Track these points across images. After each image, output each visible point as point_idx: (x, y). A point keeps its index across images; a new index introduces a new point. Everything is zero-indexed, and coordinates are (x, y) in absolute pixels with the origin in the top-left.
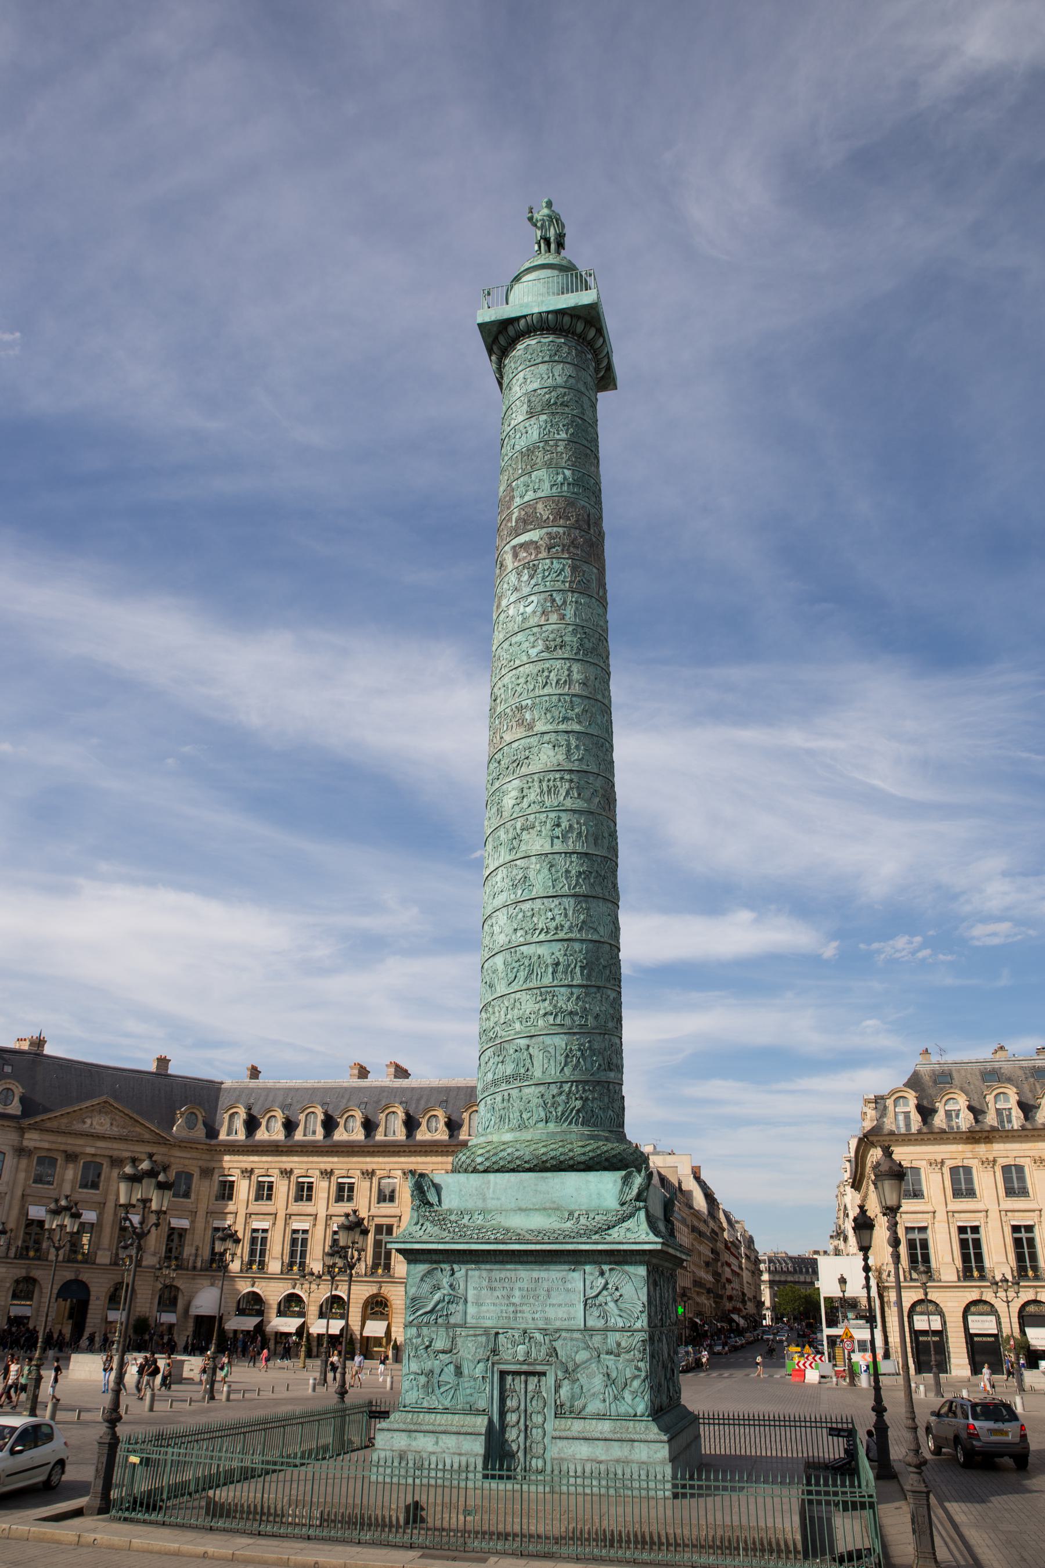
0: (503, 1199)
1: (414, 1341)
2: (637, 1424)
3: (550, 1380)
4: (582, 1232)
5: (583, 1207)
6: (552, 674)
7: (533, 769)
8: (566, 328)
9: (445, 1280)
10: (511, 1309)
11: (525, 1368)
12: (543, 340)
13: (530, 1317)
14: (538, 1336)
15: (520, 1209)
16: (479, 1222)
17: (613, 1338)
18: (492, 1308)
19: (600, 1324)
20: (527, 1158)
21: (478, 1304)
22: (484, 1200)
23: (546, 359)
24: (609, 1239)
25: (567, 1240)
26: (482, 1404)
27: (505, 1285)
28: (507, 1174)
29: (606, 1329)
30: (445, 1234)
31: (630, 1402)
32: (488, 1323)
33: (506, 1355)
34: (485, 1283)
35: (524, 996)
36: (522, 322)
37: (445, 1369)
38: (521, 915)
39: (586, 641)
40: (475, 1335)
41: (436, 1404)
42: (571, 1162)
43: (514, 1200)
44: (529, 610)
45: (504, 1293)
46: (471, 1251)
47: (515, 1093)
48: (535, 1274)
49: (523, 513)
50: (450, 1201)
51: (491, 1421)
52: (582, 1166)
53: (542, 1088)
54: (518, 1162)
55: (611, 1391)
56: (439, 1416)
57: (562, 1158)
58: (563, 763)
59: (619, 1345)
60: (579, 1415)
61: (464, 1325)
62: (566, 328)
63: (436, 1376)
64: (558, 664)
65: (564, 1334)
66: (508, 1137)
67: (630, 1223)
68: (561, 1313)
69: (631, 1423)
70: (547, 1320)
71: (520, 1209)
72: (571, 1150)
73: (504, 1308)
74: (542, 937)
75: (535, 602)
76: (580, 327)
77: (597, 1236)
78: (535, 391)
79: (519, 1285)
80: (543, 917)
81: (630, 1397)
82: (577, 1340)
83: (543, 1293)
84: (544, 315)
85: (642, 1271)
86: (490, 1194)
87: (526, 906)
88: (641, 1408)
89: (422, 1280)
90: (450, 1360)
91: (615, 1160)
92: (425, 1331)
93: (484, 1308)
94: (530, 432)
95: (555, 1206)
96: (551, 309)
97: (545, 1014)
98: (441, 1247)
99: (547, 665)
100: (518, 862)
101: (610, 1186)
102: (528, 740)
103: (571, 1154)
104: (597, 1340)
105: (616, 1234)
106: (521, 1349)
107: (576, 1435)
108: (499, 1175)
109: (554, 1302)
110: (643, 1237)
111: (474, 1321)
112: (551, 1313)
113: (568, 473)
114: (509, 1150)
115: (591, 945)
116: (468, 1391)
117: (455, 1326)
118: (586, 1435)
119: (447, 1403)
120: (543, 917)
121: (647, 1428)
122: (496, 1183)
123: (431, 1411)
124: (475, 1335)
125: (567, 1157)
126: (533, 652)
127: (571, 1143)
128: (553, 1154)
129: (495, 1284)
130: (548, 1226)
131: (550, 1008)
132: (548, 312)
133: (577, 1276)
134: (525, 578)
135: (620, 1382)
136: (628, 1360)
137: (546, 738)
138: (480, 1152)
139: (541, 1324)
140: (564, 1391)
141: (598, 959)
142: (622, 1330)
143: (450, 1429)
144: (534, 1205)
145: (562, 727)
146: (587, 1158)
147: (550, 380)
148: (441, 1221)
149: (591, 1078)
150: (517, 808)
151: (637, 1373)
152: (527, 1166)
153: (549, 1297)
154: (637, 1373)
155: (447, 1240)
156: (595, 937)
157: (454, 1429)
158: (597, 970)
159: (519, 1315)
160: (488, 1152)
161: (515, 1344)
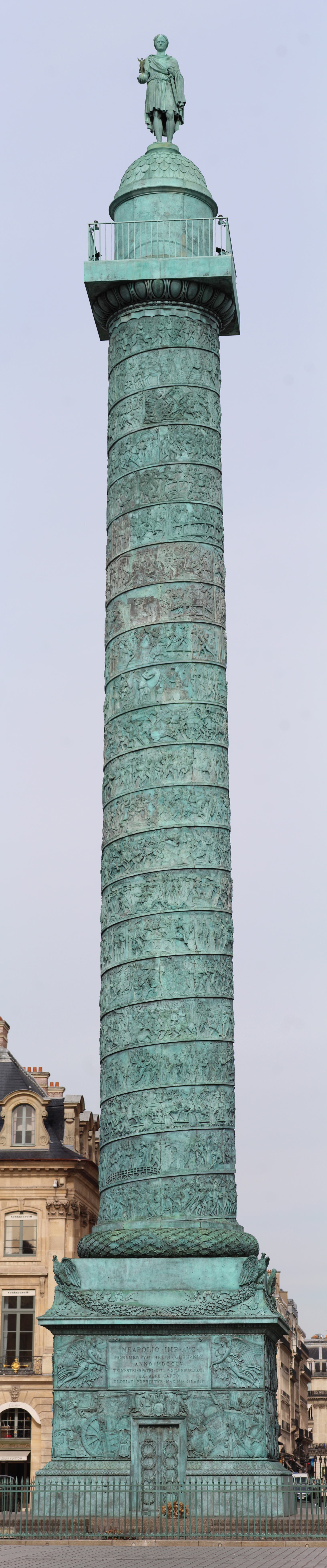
0: (138, 1280)
1: (63, 1403)
2: (255, 1463)
3: (182, 1431)
4: (210, 1309)
5: (209, 1288)
7: (157, 866)
8: (190, 298)
9: (90, 1351)
10: (148, 1374)
11: (160, 1422)
12: (163, 313)
13: (165, 1379)
14: (171, 1396)
15: (154, 1290)
16: (118, 1301)
17: (235, 1396)
18: (131, 1373)
19: (223, 1385)
20: (159, 1245)
21: (118, 1370)
22: (122, 1282)
23: (167, 343)
24: (232, 1314)
25: (198, 1315)
26: (124, 1453)
27: (143, 1354)
28: (141, 1260)
29: (229, 1389)
30: (89, 1311)
31: (249, 1446)
32: (129, 1386)
33: (146, 1411)
34: (125, 1353)
35: (151, 1095)
36: (141, 286)
37: (92, 1425)
38: (147, 1015)
39: (208, 720)
40: (117, 1397)
41: (84, 1454)
42: (197, 1249)
43: (148, 1282)
44: (151, 683)
45: (142, 1361)
46: (113, 1326)
47: (143, 1185)
48: (169, 1345)
50: (91, 1283)
51: (132, 1467)
52: (206, 1252)
53: (168, 1181)
54: (151, 1249)
55: (233, 1438)
56: (88, 1463)
57: (189, 1245)
58: (187, 862)
59: (240, 1401)
60: (207, 1458)
61: (106, 1389)
62: (190, 298)
63: (84, 1431)
65: (194, 1394)
66: (139, 1225)
67: (249, 1302)
68: (191, 1376)
69: (250, 1463)
70: (180, 1382)
71: (154, 1290)
72: (197, 1238)
73: (142, 1373)
74: (167, 1039)
75: (157, 675)
76: (206, 296)
77: (222, 1313)
79: (154, 1354)
80: (169, 1020)
81: (250, 1443)
82: (205, 1398)
83: (176, 1360)
84: (167, 283)
85: (260, 1340)
86: (126, 1276)
87: (152, 1007)
88: (259, 1450)
89: (68, 1351)
90: (96, 1417)
91: (233, 1246)
92: (72, 1394)
93: (125, 1374)
94: (149, 448)
95: (185, 1287)
96: (176, 276)
97: (170, 1114)
98: (87, 1322)
99: (170, 752)
100: (142, 963)
101: (233, 1270)
102: (152, 835)
103: (197, 1241)
104: (221, 1399)
105: (238, 1311)
106: (159, 1406)
107: (206, 1472)
108: (134, 1260)
109: (185, 1367)
110: (262, 1313)
111: (116, 1385)
112: (183, 1376)
113: (189, 507)
114: (142, 1238)
115: (211, 1046)
116: (113, 1442)
117: (99, 1389)
118: (216, 1472)
119: (94, 1453)
120: (169, 1020)
121: (263, 1466)
122: (132, 1267)
123: (79, 1459)
124: (117, 1397)
125: (193, 1244)
127: (197, 1232)
128: (181, 1241)
129: (134, 1354)
130: (180, 1304)
131: (174, 1108)
132: (172, 280)
133: (204, 1345)
134: (145, 644)
135: (242, 1430)
136: (248, 1414)
137: (170, 834)
138: (114, 1238)
139: (174, 1386)
140: (194, 1440)
141: (216, 1058)
142: (243, 1389)
143: (99, 1472)
144: (166, 1286)
145: (185, 822)
146: (210, 1245)
148: (83, 1302)
149: (211, 1171)
150: (141, 907)
151: (255, 1423)
152: (158, 1252)
153: (181, 1363)
154: (255, 1423)
155: (92, 1316)
156: (216, 1037)
157: (103, 1472)
158: (216, 1069)
159: (155, 1379)
160: (122, 1239)
161: (152, 1403)
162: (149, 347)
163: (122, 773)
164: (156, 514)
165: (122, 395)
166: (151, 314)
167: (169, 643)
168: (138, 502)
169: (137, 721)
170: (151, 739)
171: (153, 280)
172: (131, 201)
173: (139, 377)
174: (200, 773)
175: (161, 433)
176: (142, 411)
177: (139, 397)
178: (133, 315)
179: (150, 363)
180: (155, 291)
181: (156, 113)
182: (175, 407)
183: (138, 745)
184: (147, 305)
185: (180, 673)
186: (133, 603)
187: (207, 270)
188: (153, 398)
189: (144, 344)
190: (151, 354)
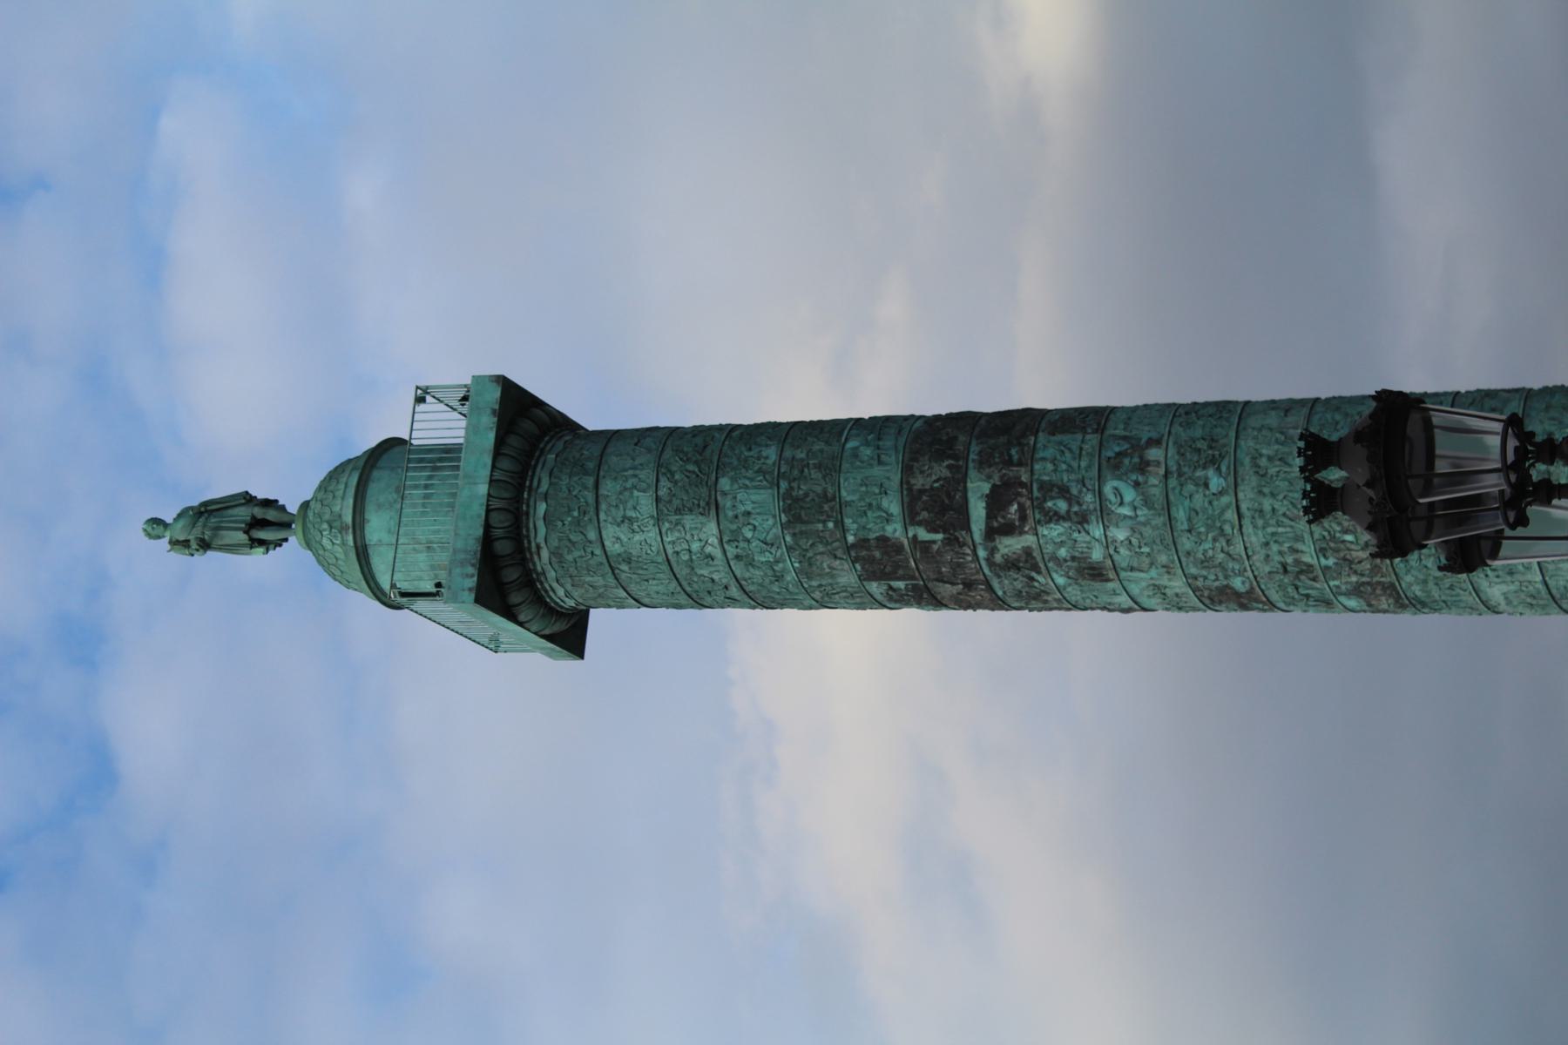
6: (1264, 451)
12: (544, 487)
23: (590, 481)
36: (496, 518)
44: (1129, 495)
49: (925, 515)
64: (1247, 444)
75: (1116, 483)
78: (658, 500)
84: (497, 475)
94: (749, 508)
96: (489, 462)
99: (1247, 461)
126: (1216, 483)
132: (494, 467)
147: (642, 474)
162: (592, 510)
163: (1275, 548)
164: (854, 492)
166: (542, 508)
167: (1064, 467)
168: (831, 525)
169: (1189, 520)
170: (1221, 493)
171: (489, 495)
173: (635, 527)
174: (1289, 419)
175: (727, 488)
176: (689, 520)
180: (506, 495)
182: (691, 467)
183: (1231, 515)
184: (527, 514)
185: (1117, 449)
186: (991, 533)
187: (489, 411)
190: (603, 506)
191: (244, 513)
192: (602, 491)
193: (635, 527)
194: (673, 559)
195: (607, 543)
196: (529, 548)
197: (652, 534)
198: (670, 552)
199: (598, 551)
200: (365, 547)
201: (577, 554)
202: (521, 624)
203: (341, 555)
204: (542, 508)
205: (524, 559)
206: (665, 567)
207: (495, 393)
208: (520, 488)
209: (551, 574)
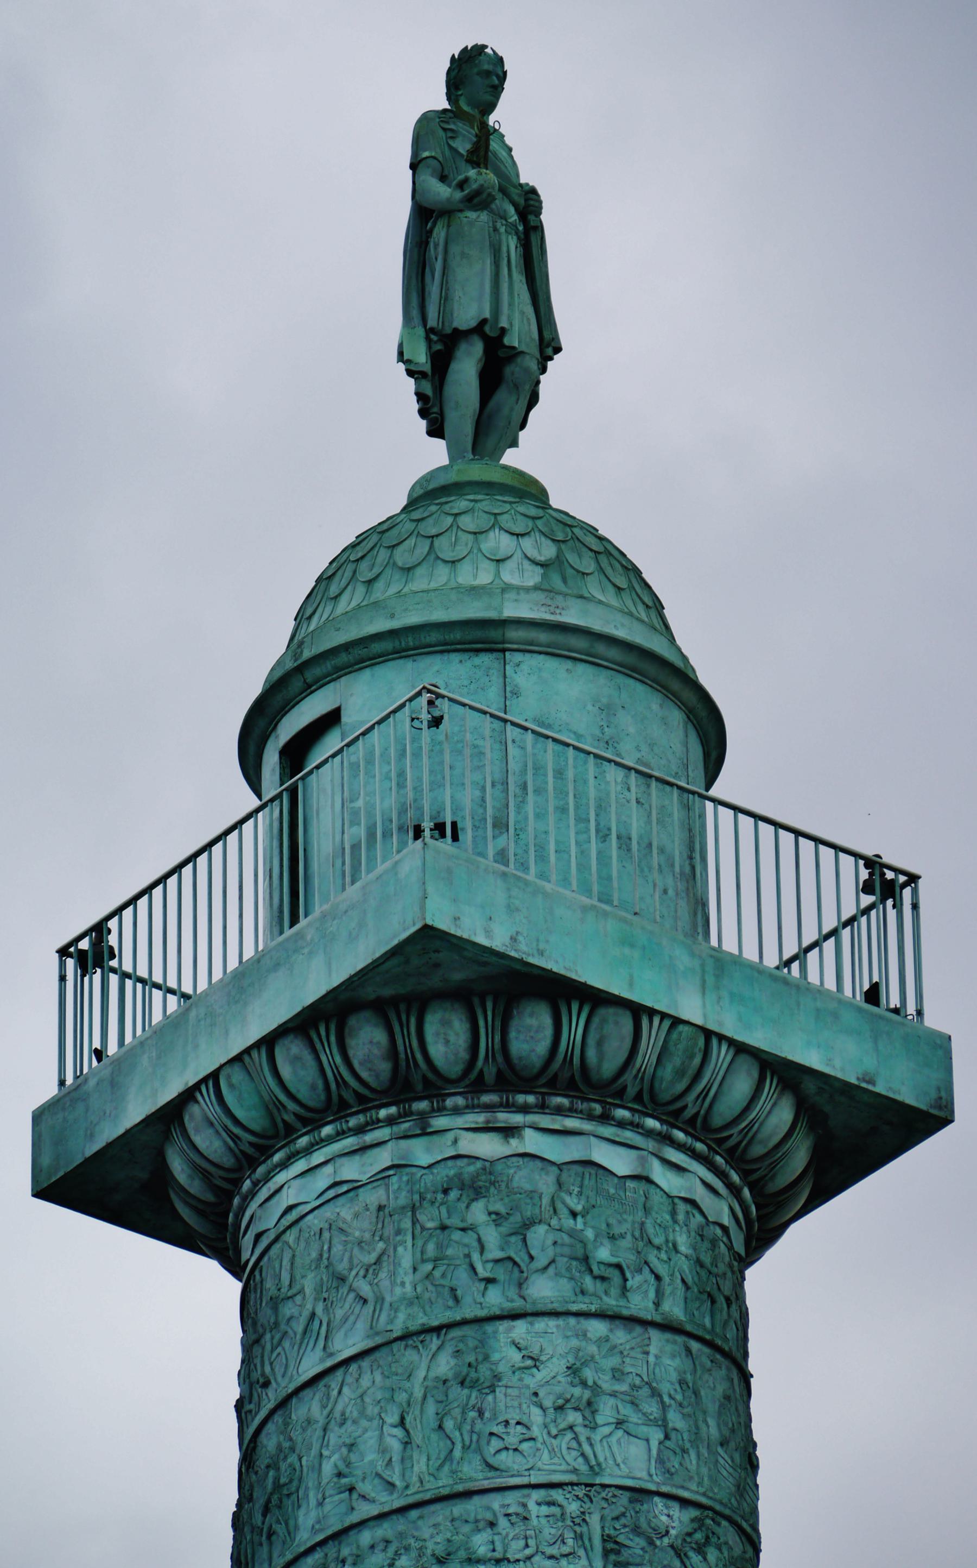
84: (722, 1055)
132: (740, 1049)
162: (611, 1302)
165: (472, 1472)
166: (619, 1162)
171: (677, 1022)
172: (485, 659)
177: (573, 1508)
178: (532, 1142)
179: (618, 1374)
181: (477, 348)
184: (605, 1118)
188: (636, 1530)
189: (588, 1281)
190: (621, 1336)
191: (520, 331)
192: (654, 1334)
193: (573, 1417)
194: (473, 1506)
195: (520, 1328)
196: (509, 1106)
197: (551, 1462)
198: (496, 1501)
199: (495, 1299)
200: (497, 648)
201: (491, 1236)
202: (268, 1042)
203: (465, 576)
204: (619, 1162)
205: (478, 1086)
206: (444, 1483)
207: (901, 1083)
208: (672, 1113)
209: (421, 1152)
